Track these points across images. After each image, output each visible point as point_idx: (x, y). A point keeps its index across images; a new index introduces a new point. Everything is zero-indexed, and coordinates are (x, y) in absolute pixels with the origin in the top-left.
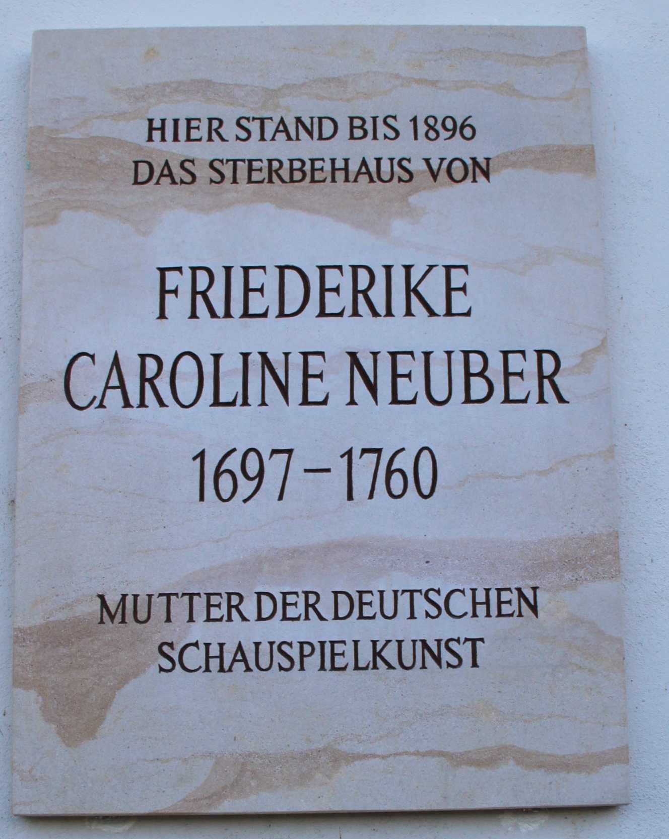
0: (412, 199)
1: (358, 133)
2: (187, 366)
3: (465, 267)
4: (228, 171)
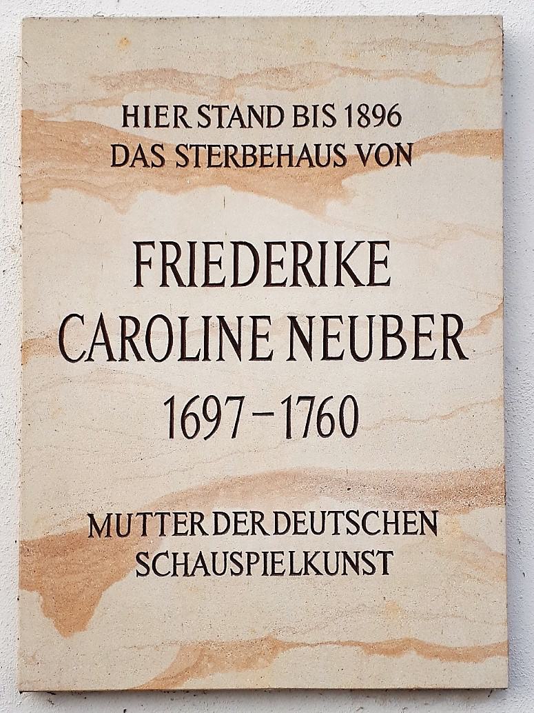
0: (345, 182)
1: (301, 121)
2: (159, 327)
3: (387, 243)
4: (191, 155)
